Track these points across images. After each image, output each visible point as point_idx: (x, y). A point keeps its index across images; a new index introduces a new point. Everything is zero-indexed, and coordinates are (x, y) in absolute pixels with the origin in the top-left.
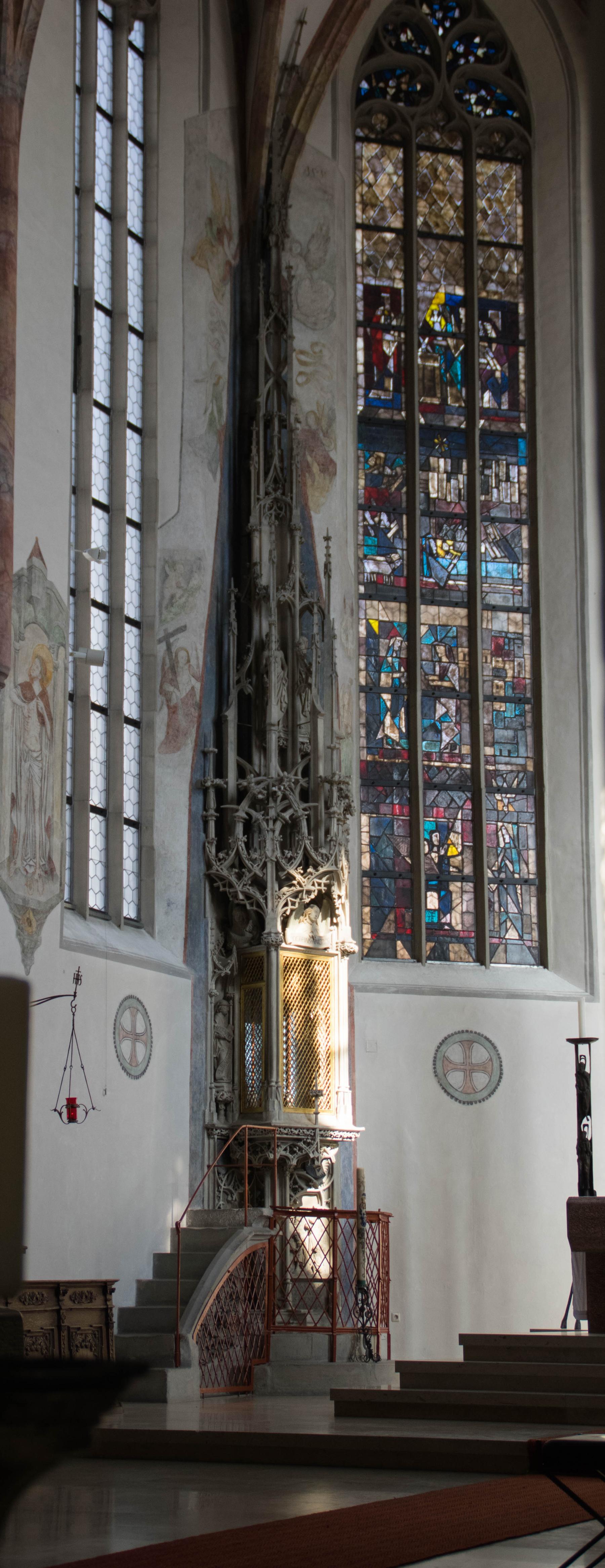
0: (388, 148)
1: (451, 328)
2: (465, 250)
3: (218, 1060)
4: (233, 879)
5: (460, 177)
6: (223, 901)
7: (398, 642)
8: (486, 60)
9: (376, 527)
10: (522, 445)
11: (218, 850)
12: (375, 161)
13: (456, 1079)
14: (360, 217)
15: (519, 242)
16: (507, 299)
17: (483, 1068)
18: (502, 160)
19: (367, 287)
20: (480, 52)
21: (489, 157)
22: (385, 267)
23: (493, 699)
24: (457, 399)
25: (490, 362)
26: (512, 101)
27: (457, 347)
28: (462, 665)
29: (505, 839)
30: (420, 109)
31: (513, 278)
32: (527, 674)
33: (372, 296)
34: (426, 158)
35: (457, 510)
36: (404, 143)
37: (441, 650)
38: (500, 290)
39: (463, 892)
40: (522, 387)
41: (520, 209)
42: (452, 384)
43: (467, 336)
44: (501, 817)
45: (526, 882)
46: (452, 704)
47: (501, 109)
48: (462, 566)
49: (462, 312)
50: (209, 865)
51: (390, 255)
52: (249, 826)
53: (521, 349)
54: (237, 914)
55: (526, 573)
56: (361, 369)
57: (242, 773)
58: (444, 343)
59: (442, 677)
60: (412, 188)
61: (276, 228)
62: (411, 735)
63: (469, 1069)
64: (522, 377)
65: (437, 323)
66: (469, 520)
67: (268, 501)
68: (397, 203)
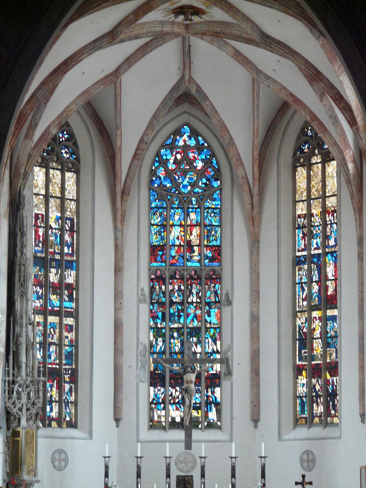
0: (41, 168)
1: (57, 227)
2: (61, 201)
3: (6, 461)
4: (13, 408)
5: (60, 177)
7: (41, 328)
9: (36, 291)
10: (74, 264)
11: (9, 399)
12: (38, 173)
14: (35, 191)
15: (75, 198)
16: (72, 217)
17: (63, 460)
18: (71, 172)
19: (35, 214)
20: (66, 136)
21: (68, 171)
22: (40, 207)
23: (65, 345)
24: (58, 250)
25: (67, 238)
26: (75, 152)
27: (58, 233)
28: (58, 335)
30: (51, 157)
31: (73, 210)
32: (74, 338)
34: (51, 171)
35: (58, 286)
36: (47, 168)
37: (52, 330)
38: (70, 214)
39: (56, 405)
40: (75, 246)
41: (75, 187)
42: (57, 245)
44: (65, 382)
45: (72, 402)
46: (54, 347)
47: (72, 154)
48: (57, 303)
49: (60, 221)
50: (5, 404)
51: (41, 203)
52: (18, 393)
53: (75, 233)
54: (12, 418)
55: (74, 306)
56: (34, 240)
57: (13, 375)
58: (55, 232)
59: (52, 339)
61: (23, 204)
62: (44, 357)
64: (75, 242)
65: (54, 225)
67: (20, 291)
68: (44, 186)
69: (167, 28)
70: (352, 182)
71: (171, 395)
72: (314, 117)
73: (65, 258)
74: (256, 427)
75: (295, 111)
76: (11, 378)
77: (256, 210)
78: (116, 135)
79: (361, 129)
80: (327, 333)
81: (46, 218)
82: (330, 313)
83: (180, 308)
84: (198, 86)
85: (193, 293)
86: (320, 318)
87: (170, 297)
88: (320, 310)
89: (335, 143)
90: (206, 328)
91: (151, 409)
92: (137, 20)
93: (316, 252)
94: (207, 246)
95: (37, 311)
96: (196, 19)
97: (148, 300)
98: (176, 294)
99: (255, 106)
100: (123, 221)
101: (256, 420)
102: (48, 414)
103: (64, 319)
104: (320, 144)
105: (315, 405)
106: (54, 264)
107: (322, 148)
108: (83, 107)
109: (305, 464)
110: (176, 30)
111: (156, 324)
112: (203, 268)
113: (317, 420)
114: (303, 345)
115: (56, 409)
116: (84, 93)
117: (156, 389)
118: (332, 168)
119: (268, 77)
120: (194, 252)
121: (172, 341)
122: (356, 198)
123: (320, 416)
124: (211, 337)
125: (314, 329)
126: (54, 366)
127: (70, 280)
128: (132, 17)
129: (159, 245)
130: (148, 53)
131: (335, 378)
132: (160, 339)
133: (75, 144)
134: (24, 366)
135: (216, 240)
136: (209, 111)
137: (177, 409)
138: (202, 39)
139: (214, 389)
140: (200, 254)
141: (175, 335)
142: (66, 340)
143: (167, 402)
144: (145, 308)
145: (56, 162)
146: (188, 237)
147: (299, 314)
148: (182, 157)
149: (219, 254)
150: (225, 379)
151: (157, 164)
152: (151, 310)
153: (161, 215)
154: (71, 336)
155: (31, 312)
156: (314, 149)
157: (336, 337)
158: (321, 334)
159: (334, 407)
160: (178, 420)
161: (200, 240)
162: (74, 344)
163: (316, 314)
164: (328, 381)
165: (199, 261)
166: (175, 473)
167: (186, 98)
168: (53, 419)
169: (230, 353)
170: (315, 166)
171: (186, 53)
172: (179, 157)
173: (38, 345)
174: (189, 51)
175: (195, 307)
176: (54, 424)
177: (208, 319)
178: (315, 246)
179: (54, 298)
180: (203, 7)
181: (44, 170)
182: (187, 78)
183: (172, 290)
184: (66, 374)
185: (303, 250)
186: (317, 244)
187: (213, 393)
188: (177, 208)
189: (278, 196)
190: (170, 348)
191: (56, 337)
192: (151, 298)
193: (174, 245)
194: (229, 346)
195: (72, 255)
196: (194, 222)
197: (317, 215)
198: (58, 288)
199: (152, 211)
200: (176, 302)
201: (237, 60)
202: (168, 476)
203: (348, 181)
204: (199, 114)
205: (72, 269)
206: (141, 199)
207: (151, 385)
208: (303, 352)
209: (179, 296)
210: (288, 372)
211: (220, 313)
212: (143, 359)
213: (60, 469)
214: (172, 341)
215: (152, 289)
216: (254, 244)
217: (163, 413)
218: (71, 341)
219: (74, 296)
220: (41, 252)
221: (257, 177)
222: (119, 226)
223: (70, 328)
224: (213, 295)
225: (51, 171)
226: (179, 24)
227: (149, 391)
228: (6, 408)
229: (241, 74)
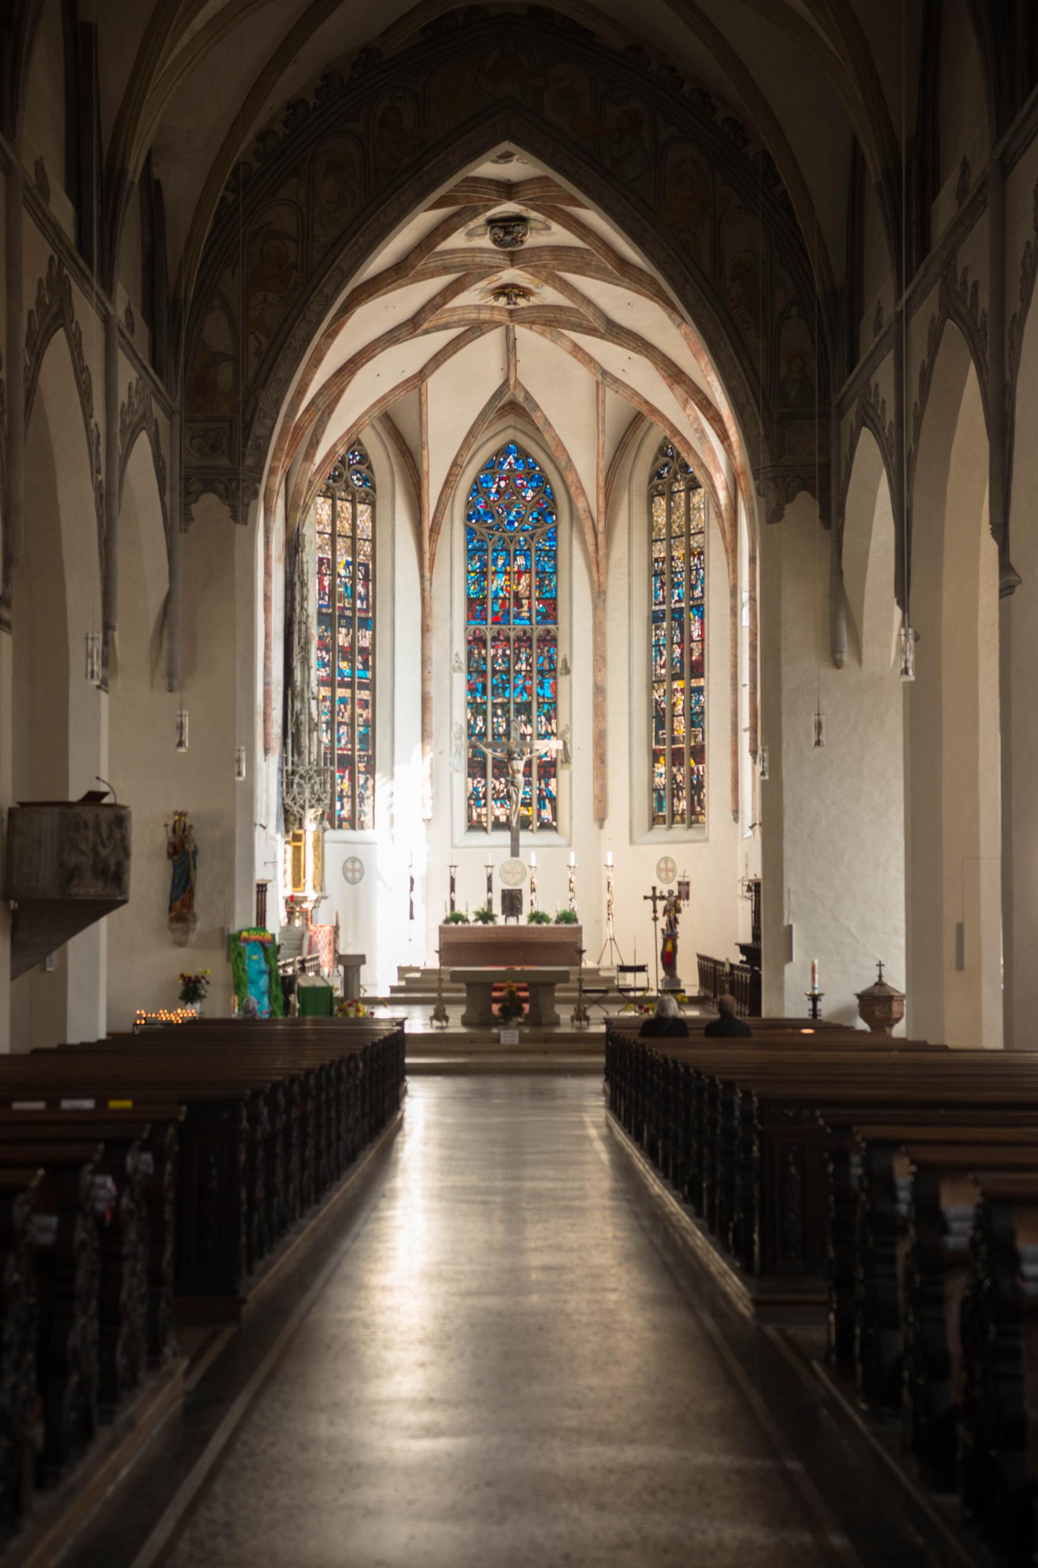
5: (350, 510)
6: (286, 812)
7: (328, 703)
8: (359, 463)
11: (287, 793)
13: (349, 875)
20: (358, 458)
21: (360, 502)
25: (360, 589)
29: (362, 781)
30: (338, 484)
32: (370, 716)
33: (321, 560)
34: (339, 503)
36: (333, 498)
37: (342, 706)
43: (353, 577)
44: (359, 772)
47: (364, 483)
48: (347, 671)
50: (283, 799)
52: (299, 785)
54: (292, 818)
57: (293, 763)
60: (335, 516)
62: (332, 741)
63: (354, 871)
65: (342, 572)
66: (353, 654)
69: (485, 315)
70: (724, 515)
71: (494, 788)
72: (676, 432)
73: (358, 614)
74: (601, 827)
75: (651, 424)
76: (290, 767)
77: (601, 553)
78: (422, 456)
79: (735, 445)
80: (692, 709)
81: (332, 564)
82: (694, 683)
83: (504, 677)
84: (527, 392)
85: (520, 659)
86: (682, 690)
87: (493, 665)
88: (683, 679)
89: (702, 466)
90: (539, 704)
91: (470, 806)
92: (445, 303)
93: (678, 605)
94: (538, 599)
95: (322, 683)
96: (522, 302)
97: (464, 668)
98: (500, 661)
99: (599, 418)
100: (431, 567)
101: (601, 819)
102: (337, 813)
103: (357, 692)
104: (685, 467)
105: (675, 800)
106: (343, 621)
107: (687, 473)
108: (379, 419)
109: (663, 874)
110: (497, 317)
111: (475, 698)
112: (534, 627)
113: (678, 818)
114: (660, 724)
115: (348, 806)
116: (379, 401)
117: (475, 782)
118: (697, 499)
119: (616, 380)
120: (522, 606)
121: (495, 720)
122: (728, 536)
123: (682, 814)
124: (544, 715)
125: (674, 704)
126: (345, 752)
127: (365, 643)
128: (438, 299)
129: (478, 598)
130: (461, 348)
131: (701, 767)
132: (480, 718)
133: (370, 468)
134: (307, 752)
135: (550, 591)
136: (540, 424)
137: (502, 806)
138: (531, 329)
139: (549, 778)
140: (530, 610)
141: (499, 712)
142: (361, 719)
143: (489, 797)
144: (460, 680)
145: (345, 491)
146: (515, 587)
147: (656, 685)
148: (507, 484)
149: (555, 609)
150: (562, 767)
151: (475, 494)
152: (469, 681)
153: (480, 558)
154: (366, 713)
155: (314, 683)
156: (676, 473)
157: (702, 713)
158: (683, 709)
159: (701, 802)
160: (503, 819)
161: (530, 591)
162: (371, 723)
163: (677, 685)
164: (692, 769)
165: (530, 618)
166: (498, 886)
167: (510, 406)
168: (345, 819)
169: (568, 735)
170: (677, 495)
171: (510, 347)
172: (503, 484)
173: (324, 726)
174: (515, 346)
175: (524, 676)
176: (345, 824)
177: (541, 693)
178: (676, 598)
179: (344, 665)
180: (531, 286)
181: (330, 501)
182: (512, 382)
183: (495, 656)
184: (360, 762)
185: (661, 603)
186: (679, 595)
187: (547, 785)
188: (501, 551)
189: (629, 533)
190: (493, 729)
191: (347, 715)
192: (469, 667)
193: (496, 598)
194: (567, 726)
195: (366, 611)
196: (523, 568)
197: (679, 559)
198: (348, 654)
199: (471, 554)
200: (499, 671)
201: (576, 357)
202: (490, 889)
203: (719, 515)
204: (528, 428)
205: (367, 629)
206: (454, 540)
207: (469, 776)
208: (660, 733)
209: (504, 662)
210: (642, 759)
211: (556, 683)
212: (459, 742)
213: (353, 882)
214: (495, 720)
215: (470, 654)
216: (599, 596)
217: (484, 811)
218: (366, 720)
219: (370, 663)
220: (328, 607)
221: (602, 509)
222: (427, 574)
223: (364, 704)
224: (546, 661)
225: (339, 503)
226: (500, 309)
227: (467, 783)
228: (284, 805)
229: (582, 376)
